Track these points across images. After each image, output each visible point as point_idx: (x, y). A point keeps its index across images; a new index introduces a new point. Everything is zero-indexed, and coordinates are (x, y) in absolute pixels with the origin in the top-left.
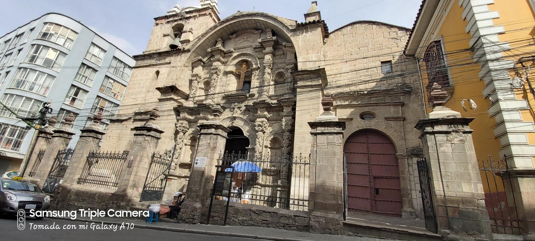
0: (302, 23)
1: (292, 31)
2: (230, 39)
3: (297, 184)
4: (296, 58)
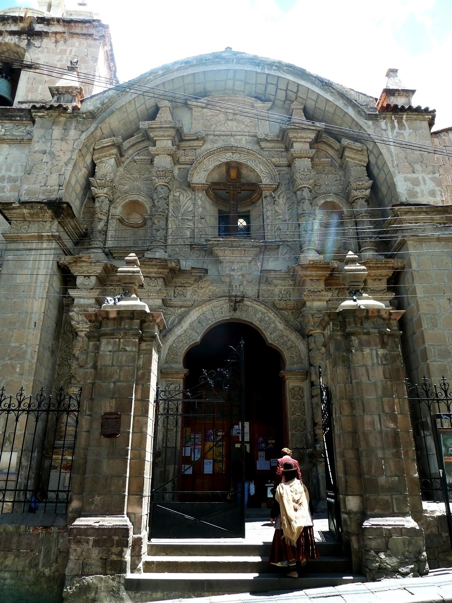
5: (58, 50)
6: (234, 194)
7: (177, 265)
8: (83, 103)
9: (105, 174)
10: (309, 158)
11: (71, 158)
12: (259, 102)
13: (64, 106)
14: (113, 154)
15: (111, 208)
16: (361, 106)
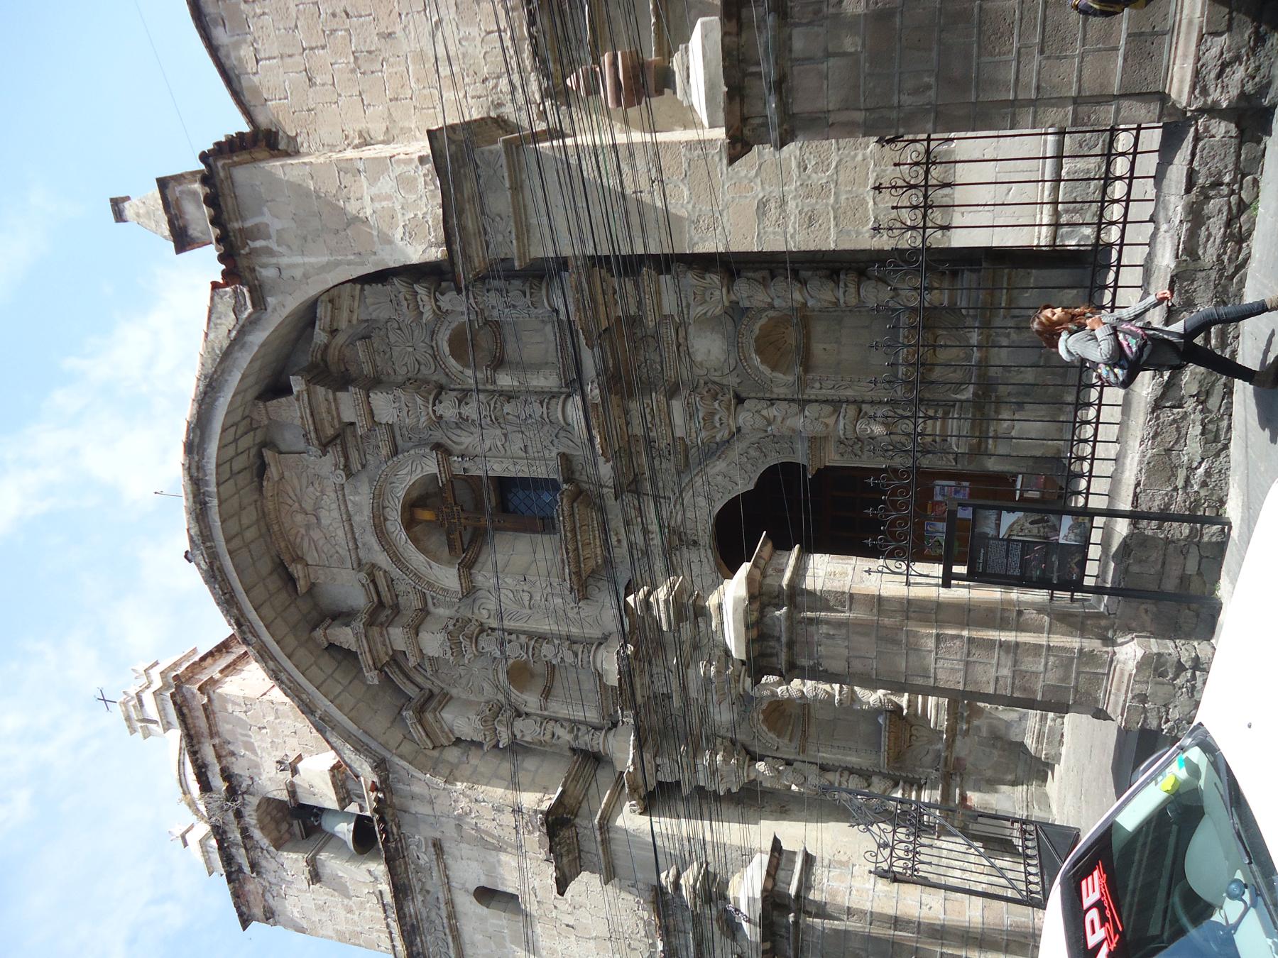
0: (222, 259)
1: (259, 302)
2: (312, 586)
3: (984, 217)
4: (382, 276)
12: (268, 473)
16: (241, 323)
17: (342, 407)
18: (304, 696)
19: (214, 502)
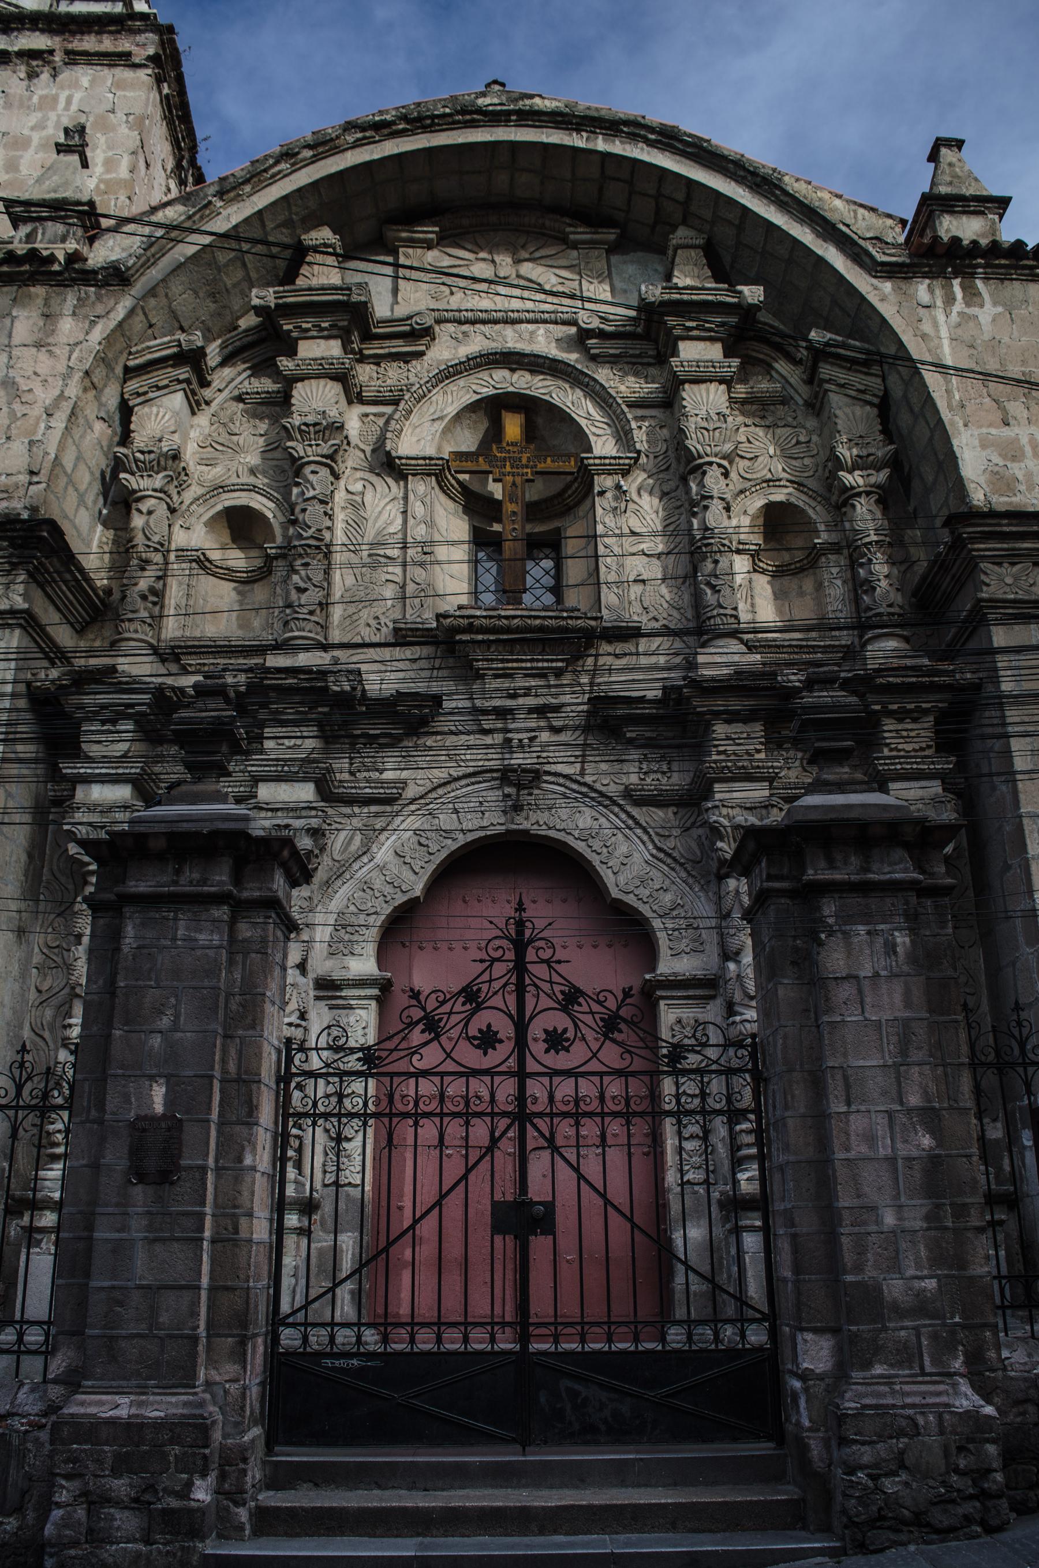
5: (35, 99)
6: (514, 484)
7: (354, 689)
8: (96, 245)
9: (158, 436)
10: (721, 382)
11: (61, 396)
13: (45, 253)
14: (179, 382)
15: (176, 528)
16: (861, 242)
17: (700, 345)
18: (248, 188)
19: (578, 141)
